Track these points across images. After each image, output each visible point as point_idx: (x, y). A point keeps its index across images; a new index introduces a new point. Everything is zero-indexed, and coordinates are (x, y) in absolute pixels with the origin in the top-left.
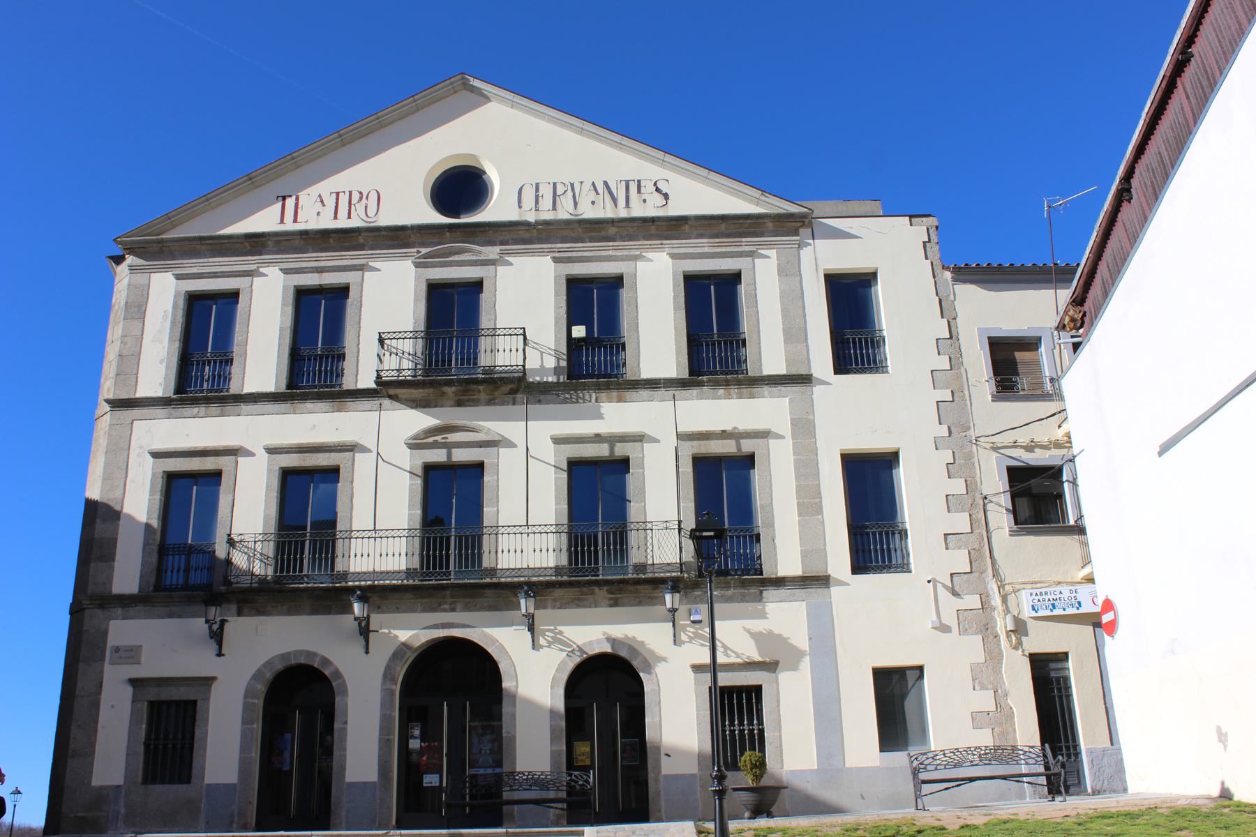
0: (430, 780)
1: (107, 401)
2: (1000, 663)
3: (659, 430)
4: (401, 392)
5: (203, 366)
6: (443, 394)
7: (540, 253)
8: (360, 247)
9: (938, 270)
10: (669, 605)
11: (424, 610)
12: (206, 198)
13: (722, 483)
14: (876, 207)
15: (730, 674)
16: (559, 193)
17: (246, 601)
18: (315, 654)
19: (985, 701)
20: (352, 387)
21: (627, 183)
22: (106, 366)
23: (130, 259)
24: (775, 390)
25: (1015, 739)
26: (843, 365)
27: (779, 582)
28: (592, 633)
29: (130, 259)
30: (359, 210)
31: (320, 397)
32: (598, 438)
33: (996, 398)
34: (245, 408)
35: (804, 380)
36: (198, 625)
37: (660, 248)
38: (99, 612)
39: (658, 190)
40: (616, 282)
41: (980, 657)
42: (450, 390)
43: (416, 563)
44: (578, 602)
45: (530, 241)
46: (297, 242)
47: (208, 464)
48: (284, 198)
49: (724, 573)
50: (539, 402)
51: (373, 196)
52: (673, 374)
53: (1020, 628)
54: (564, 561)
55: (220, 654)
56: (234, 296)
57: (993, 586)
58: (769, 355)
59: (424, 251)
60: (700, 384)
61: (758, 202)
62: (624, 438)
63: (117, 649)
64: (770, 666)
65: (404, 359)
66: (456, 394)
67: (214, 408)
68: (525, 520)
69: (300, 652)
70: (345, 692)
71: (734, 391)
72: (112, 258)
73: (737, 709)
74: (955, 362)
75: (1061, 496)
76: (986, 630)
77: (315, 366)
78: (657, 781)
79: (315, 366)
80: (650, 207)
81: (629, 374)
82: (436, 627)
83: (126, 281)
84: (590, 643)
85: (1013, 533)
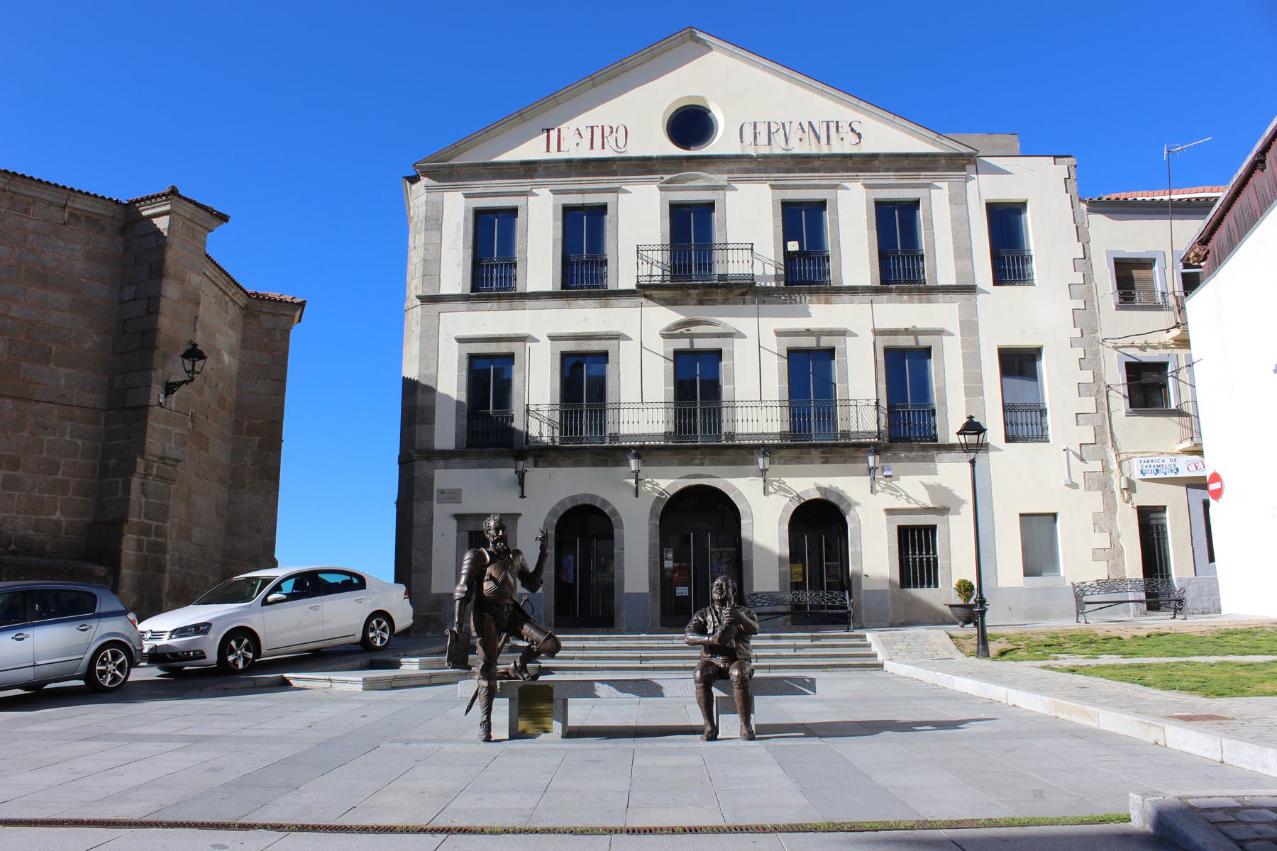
0: (682, 591)
1: (418, 297)
2: (1115, 512)
3: (858, 329)
4: (656, 293)
5: (492, 271)
6: (688, 295)
7: (760, 180)
8: (614, 173)
9: (1076, 202)
10: (871, 465)
11: (680, 464)
12: (486, 130)
13: (906, 367)
14: (1013, 142)
15: (913, 516)
16: (773, 130)
17: (541, 456)
18: (597, 497)
19: (1103, 541)
20: (615, 288)
21: (828, 124)
22: (410, 268)
23: (424, 181)
24: (947, 296)
25: (1124, 571)
26: (1000, 278)
27: (950, 448)
28: (807, 483)
29: (424, 181)
30: (610, 141)
31: (589, 296)
32: (809, 332)
33: (1118, 308)
34: (529, 303)
35: (970, 289)
36: (508, 473)
37: (856, 179)
38: (425, 463)
39: (852, 130)
40: (822, 205)
41: (1100, 508)
42: (693, 292)
43: (671, 428)
44: (798, 460)
45: (751, 171)
46: (563, 168)
47: (503, 348)
48: (548, 131)
49: (908, 440)
50: (764, 302)
51: (622, 131)
52: (868, 282)
53: (1131, 487)
54: (787, 428)
55: (522, 496)
56: (513, 211)
57: (1111, 454)
58: (942, 269)
59: (667, 177)
60: (889, 291)
61: (933, 143)
62: (830, 333)
63: (442, 492)
64: (943, 511)
65: (655, 268)
66: (698, 295)
67: (504, 304)
68: (755, 394)
69: (586, 495)
70: (621, 526)
71: (916, 297)
72: (407, 178)
73: (917, 546)
74: (1088, 278)
75: (1165, 386)
76: (1105, 487)
77: (583, 270)
78: (859, 594)
79: (583, 270)
80: (844, 145)
81: (833, 280)
82: (689, 477)
83: (423, 198)
84: (808, 491)
85: (1128, 414)
